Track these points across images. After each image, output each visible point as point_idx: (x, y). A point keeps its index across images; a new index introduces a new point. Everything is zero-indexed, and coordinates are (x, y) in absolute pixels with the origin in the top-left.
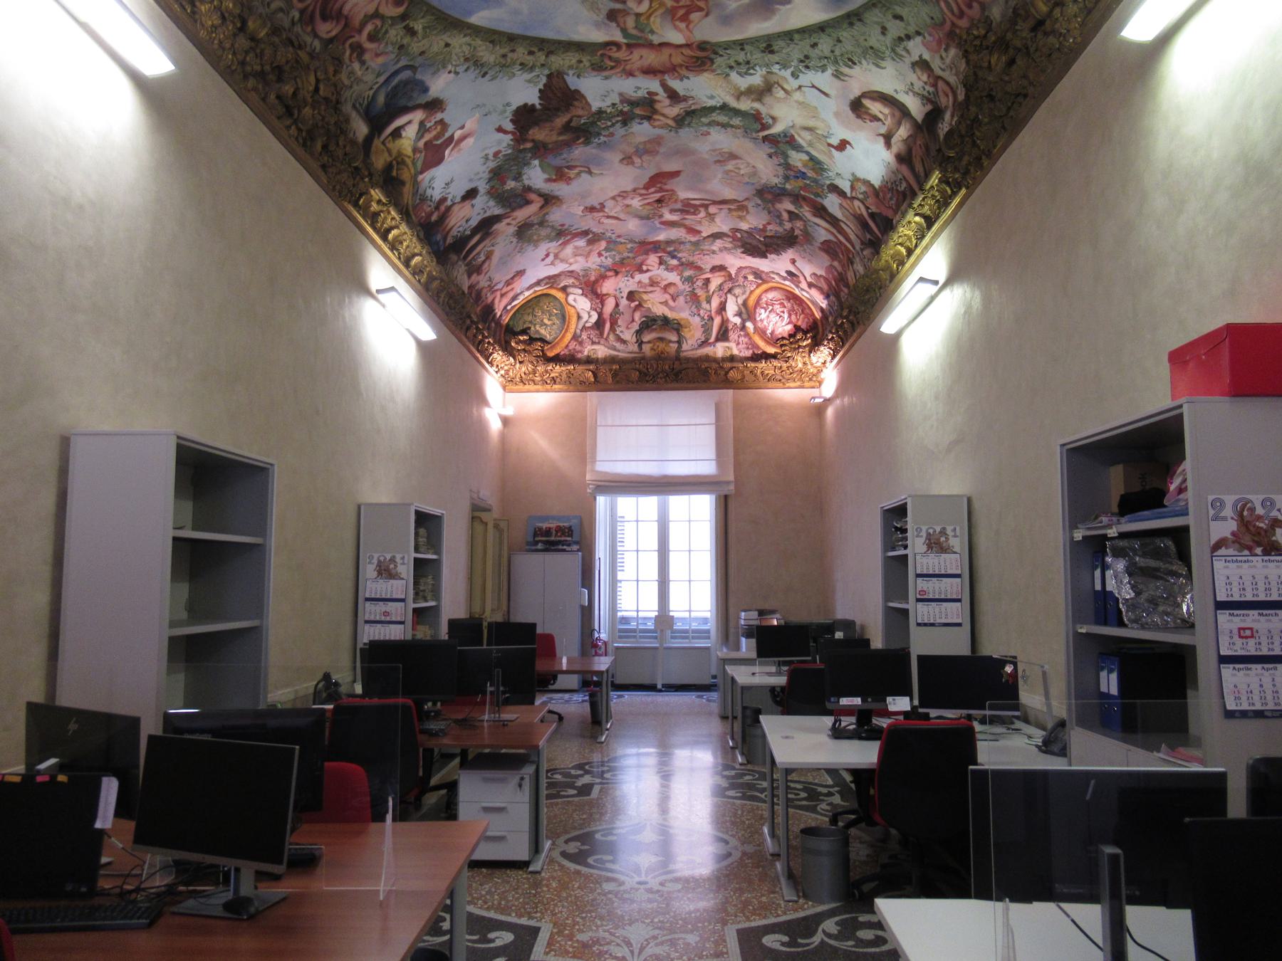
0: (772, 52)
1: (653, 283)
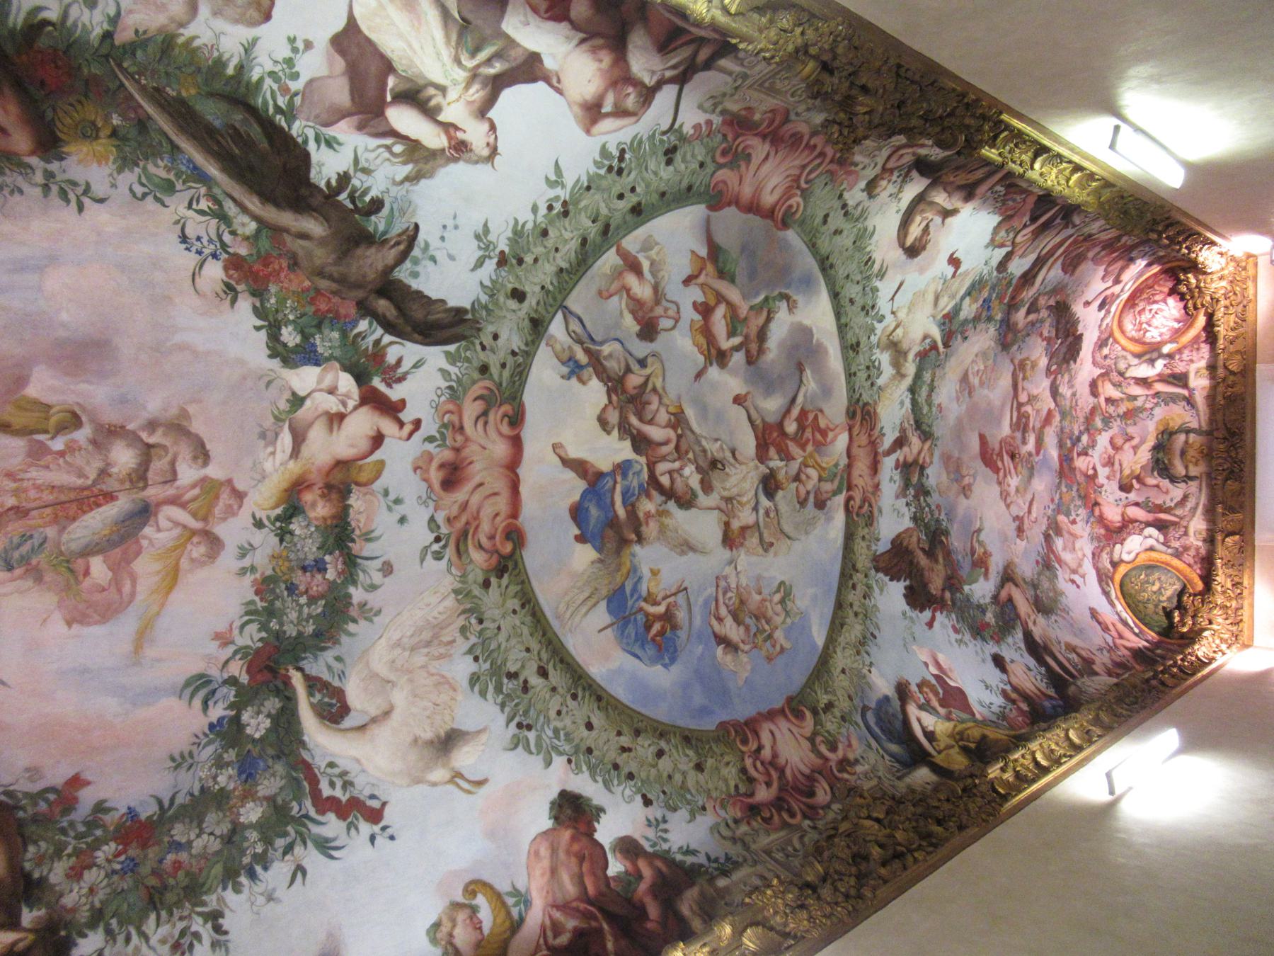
0: (858, 344)
1: (1110, 462)
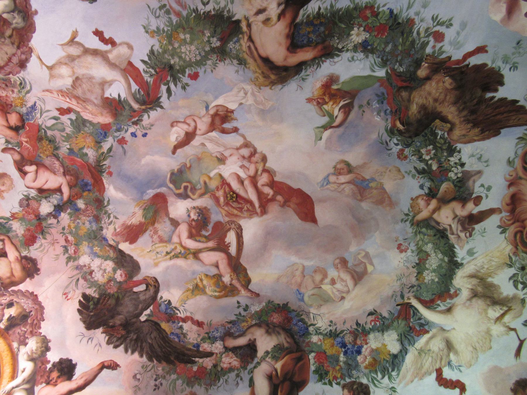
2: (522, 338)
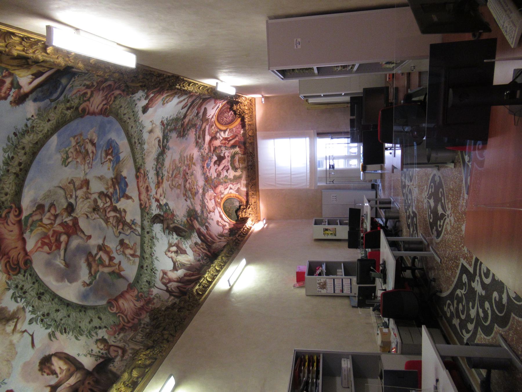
0: (39, 298)
2: (31, 334)
